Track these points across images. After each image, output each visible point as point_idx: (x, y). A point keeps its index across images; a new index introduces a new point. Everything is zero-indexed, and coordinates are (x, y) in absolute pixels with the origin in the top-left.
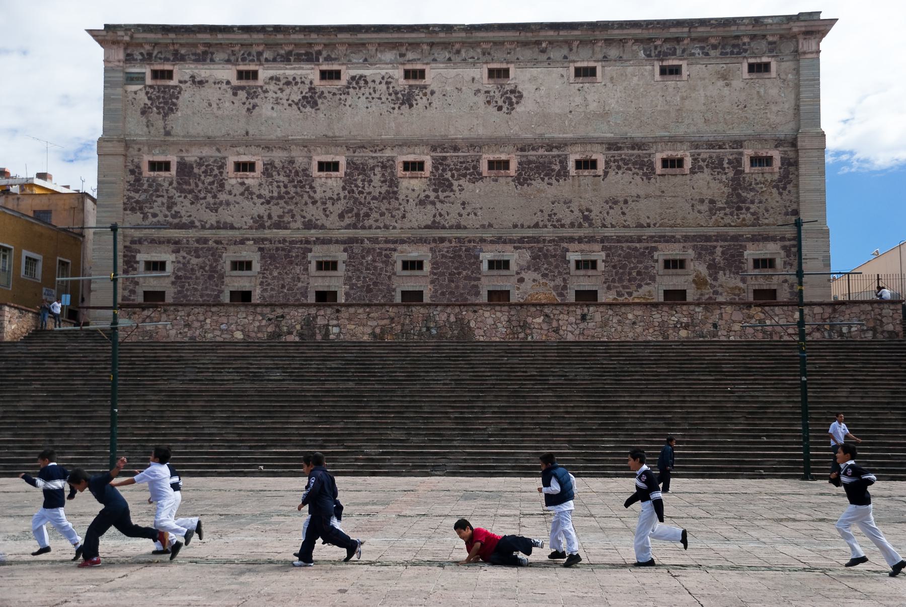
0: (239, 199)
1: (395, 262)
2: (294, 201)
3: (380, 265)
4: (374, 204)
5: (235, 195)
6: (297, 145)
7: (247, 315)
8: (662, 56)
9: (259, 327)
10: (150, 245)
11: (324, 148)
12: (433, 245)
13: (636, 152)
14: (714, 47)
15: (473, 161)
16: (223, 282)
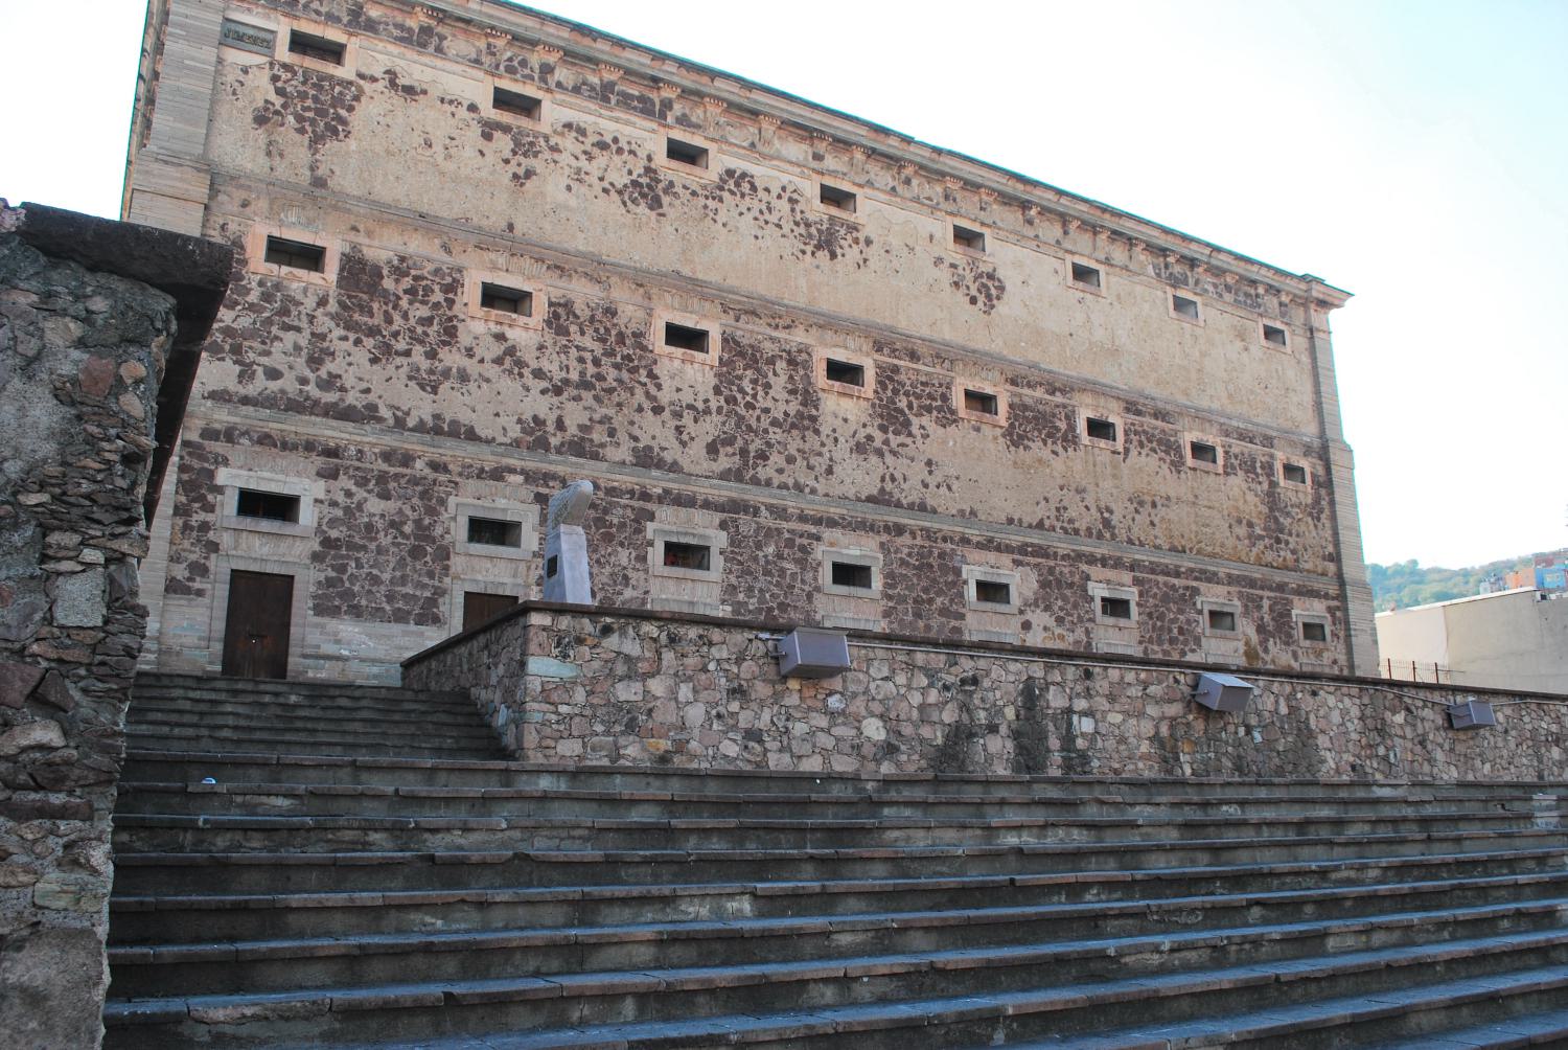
0: (492, 371)
1: (819, 564)
2: (615, 398)
3: (790, 567)
4: (776, 435)
5: (482, 361)
6: (620, 274)
7: (894, 671)
8: (1176, 281)
9: (922, 708)
10: (258, 448)
11: (677, 299)
12: (885, 538)
13: (1159, 423)
14: (1228, 288)
15: (941, 385)
16: (446, 568)
